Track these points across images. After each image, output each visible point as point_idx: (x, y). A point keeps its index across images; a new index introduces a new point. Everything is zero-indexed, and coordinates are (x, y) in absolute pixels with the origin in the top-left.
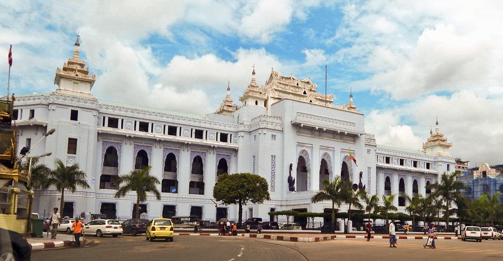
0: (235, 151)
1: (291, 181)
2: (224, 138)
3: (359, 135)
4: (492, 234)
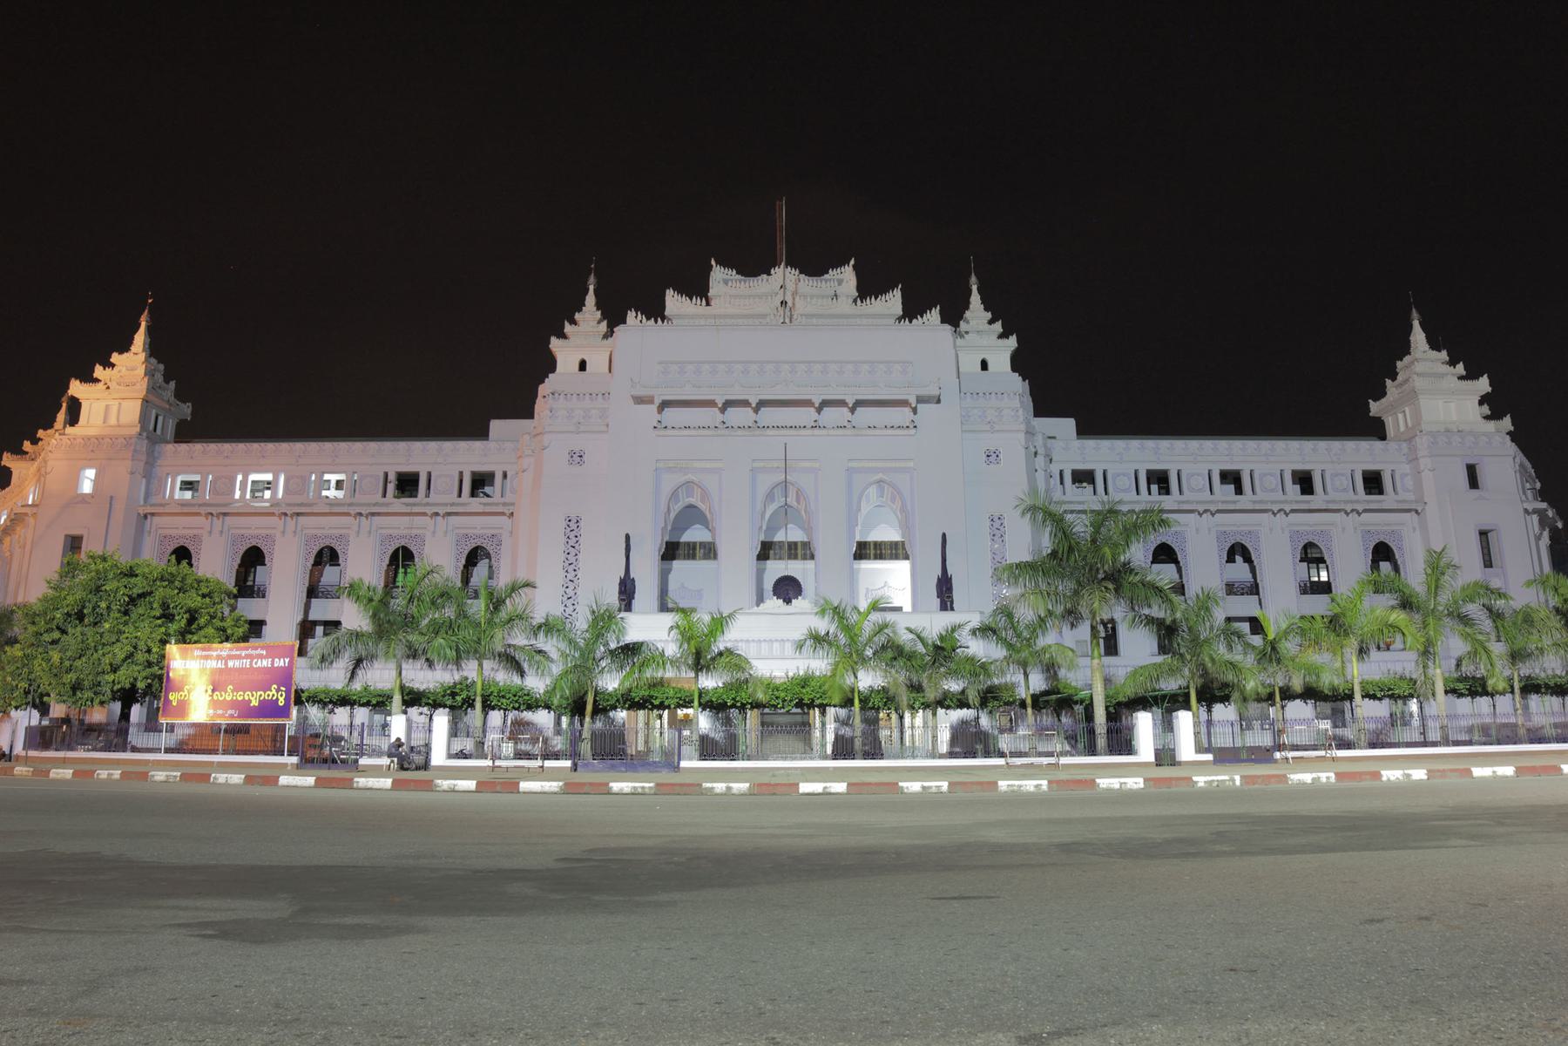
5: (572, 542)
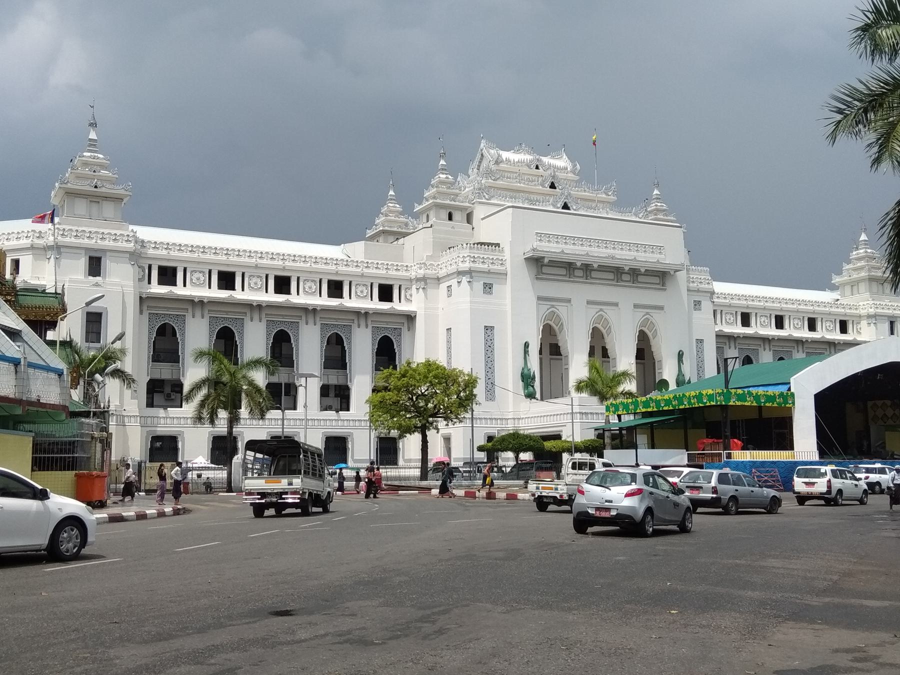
0: (410, 318)
1: (527, 379)
2: (386, 293)
3: (672, 273)
5: (489, 344)
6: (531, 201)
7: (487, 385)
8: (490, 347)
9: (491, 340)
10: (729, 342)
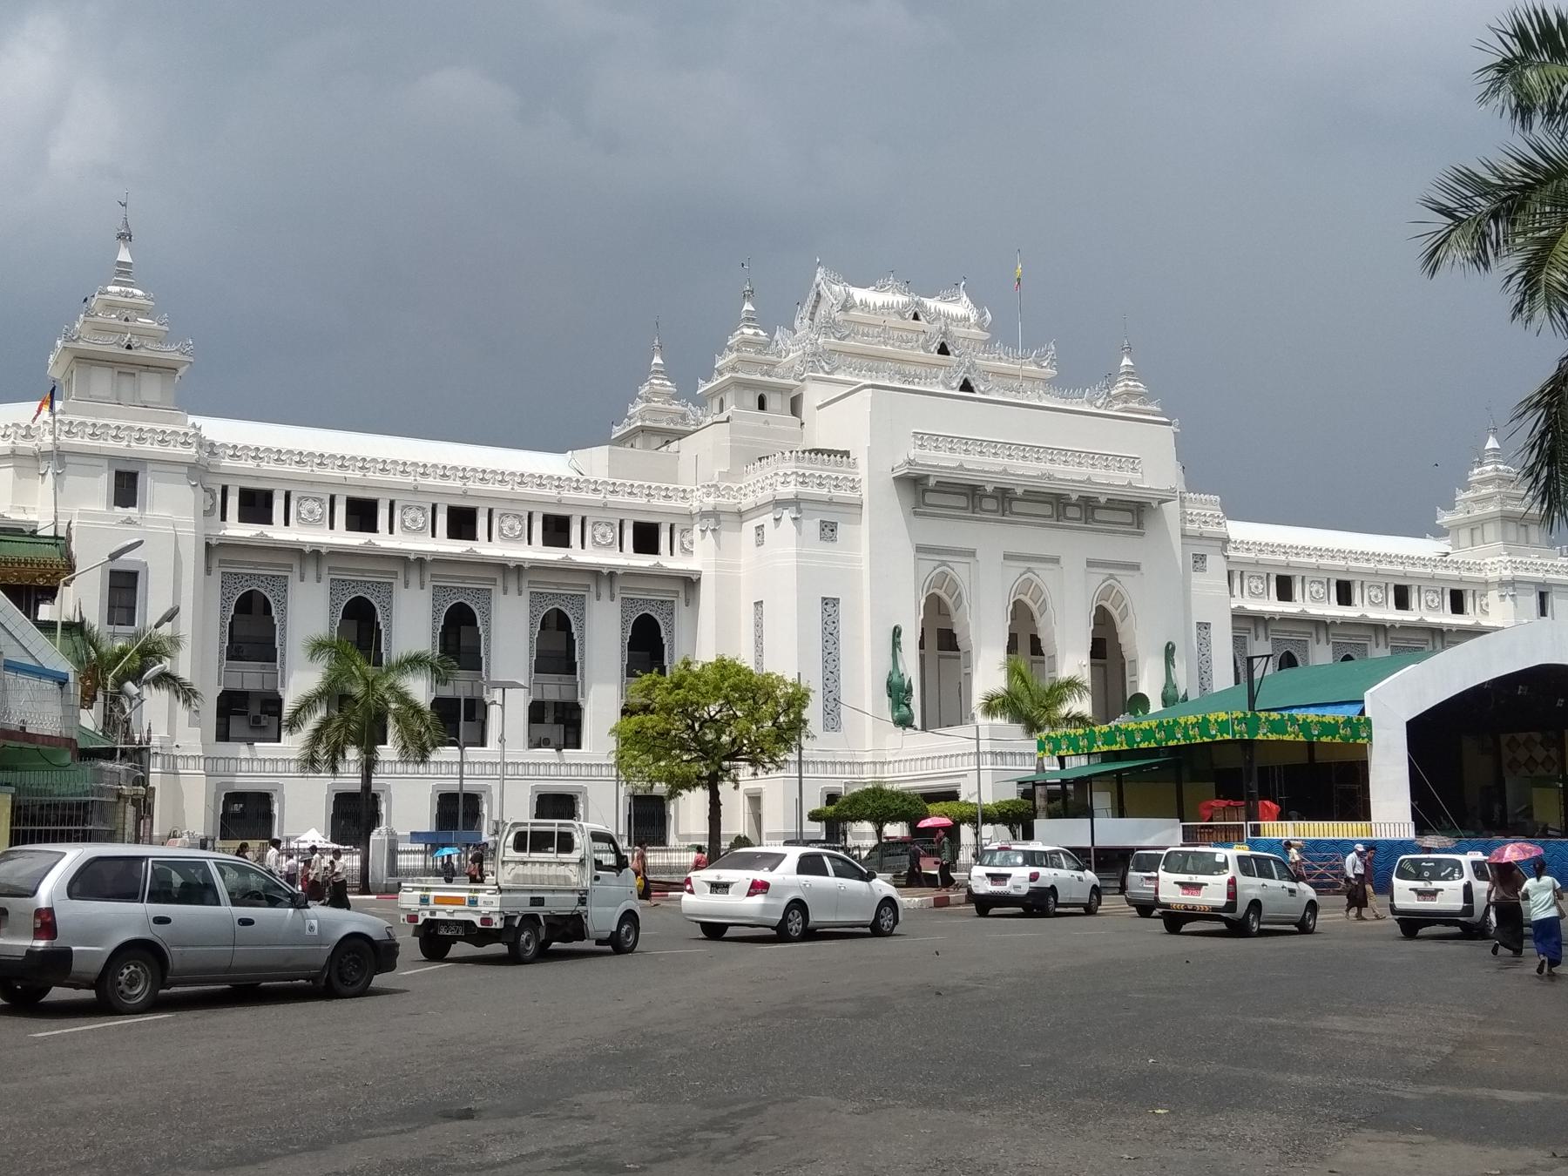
0: (690, 583)
1: (897, 692)
2: (646, 539)
3: (1155, 504)
4: (1232, 893)
6: (905, 377)
7: (826, 703)
8: (832, 634)
9: (834, 622)
10: (1433, 638)
